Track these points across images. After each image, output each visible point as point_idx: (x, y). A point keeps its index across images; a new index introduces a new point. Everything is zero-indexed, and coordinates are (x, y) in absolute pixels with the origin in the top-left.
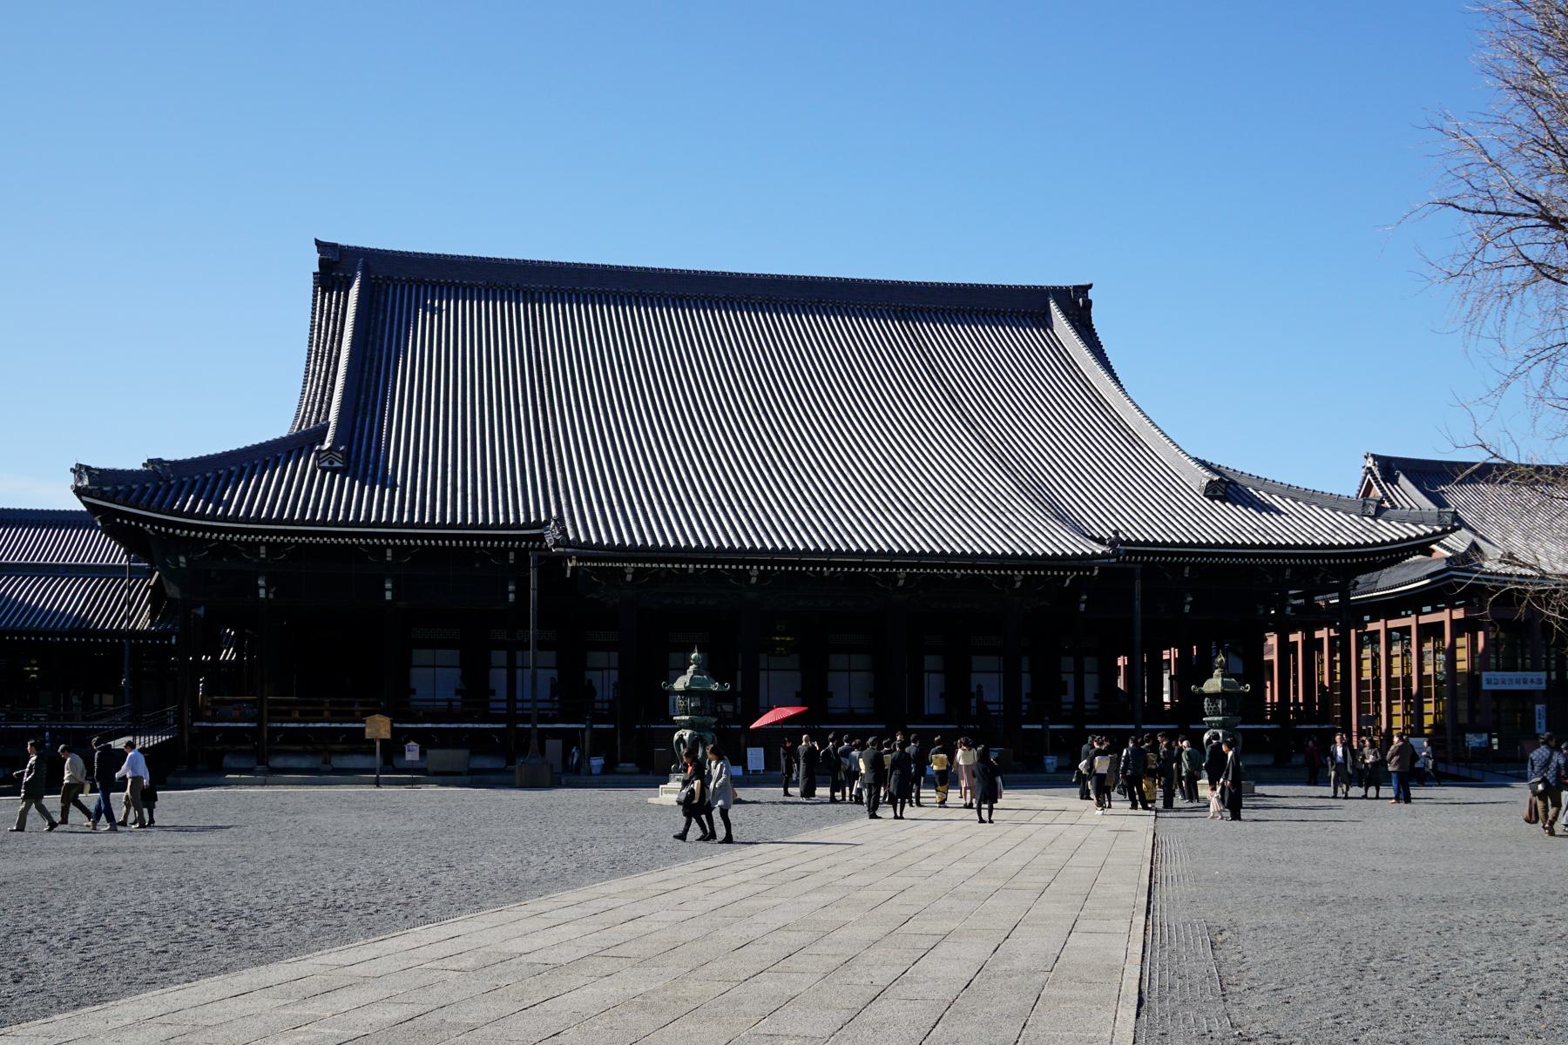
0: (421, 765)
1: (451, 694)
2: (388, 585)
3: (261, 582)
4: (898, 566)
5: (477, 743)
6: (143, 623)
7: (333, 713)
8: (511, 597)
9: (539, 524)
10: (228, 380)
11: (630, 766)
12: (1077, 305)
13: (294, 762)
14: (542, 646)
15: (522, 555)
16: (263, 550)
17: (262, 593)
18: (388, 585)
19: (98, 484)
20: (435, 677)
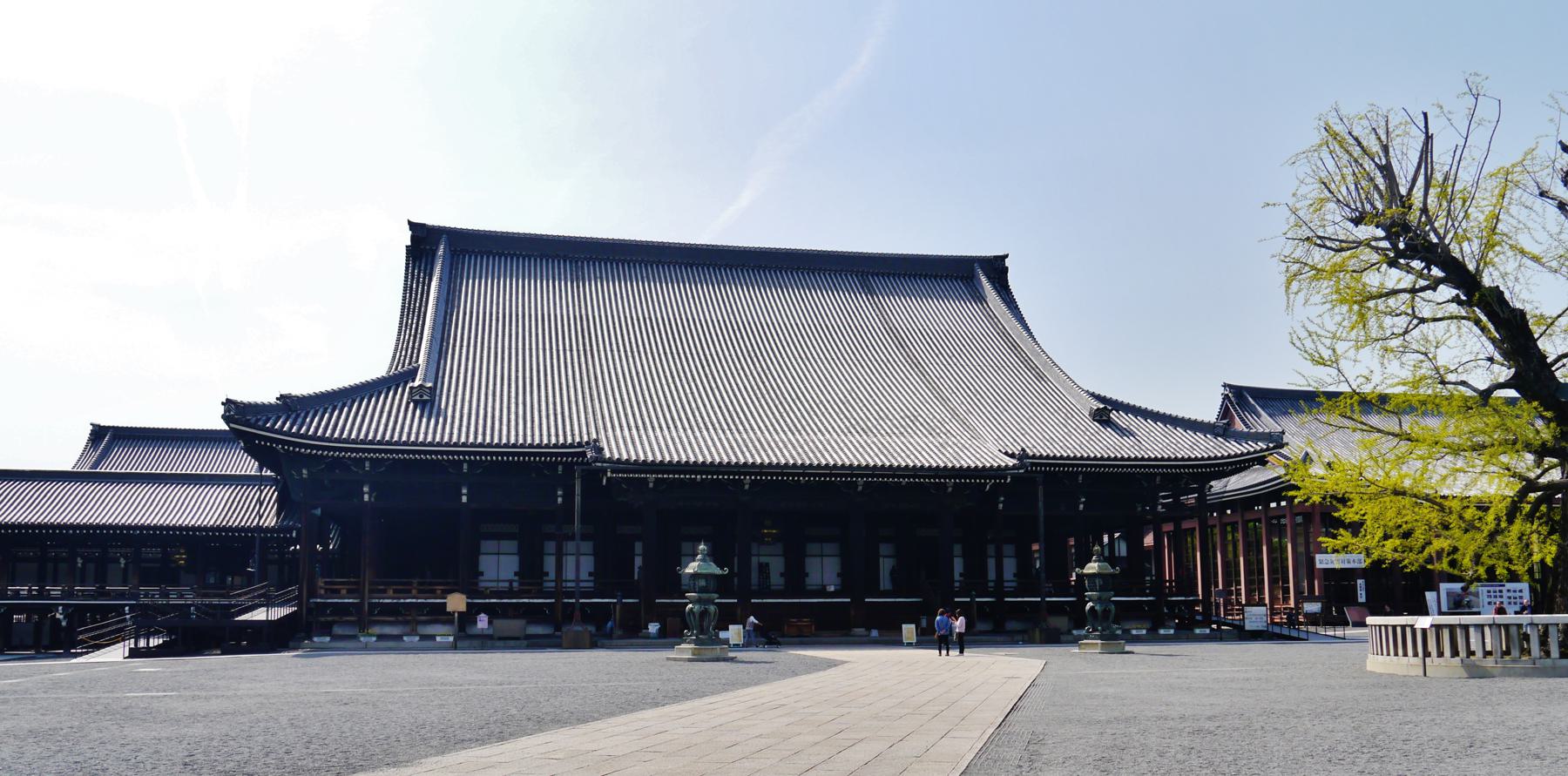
0: (491, 632)
1: (511, 576)
2: (464, 491)
4: (857, 476)
5: (532, 614)
6: (270, 520)
7: (420, 591)
9: (580, 445)
10: (332, 333)
12: (996, 269)
14: (584, 538)
15: (569, 467)
17: (366, 497)
18: (464, 491)
19: (235, 411)
20: (499, 566)
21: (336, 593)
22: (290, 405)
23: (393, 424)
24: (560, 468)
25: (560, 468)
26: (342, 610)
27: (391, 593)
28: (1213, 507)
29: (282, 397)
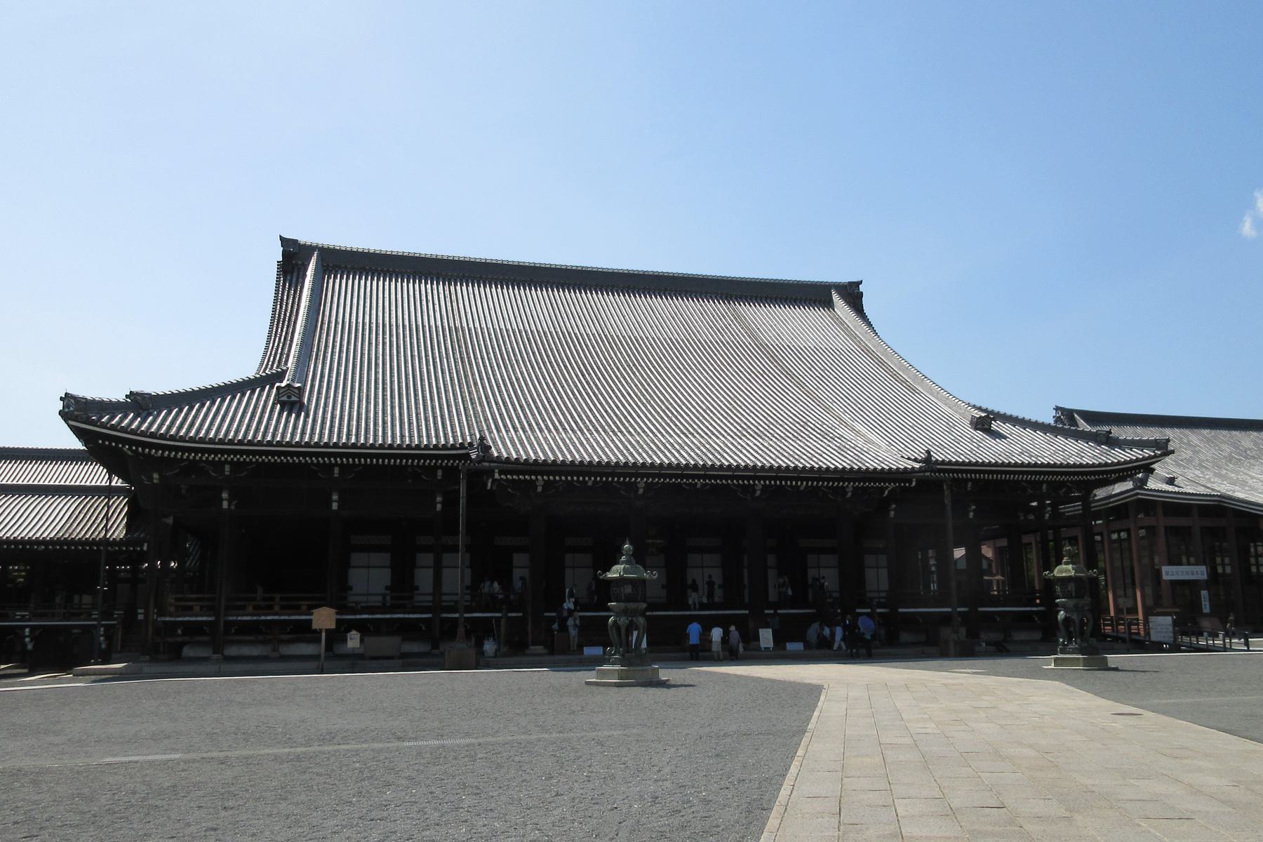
0: (361, 651)
2: (335, 497)
3: (225, 495)
5: (406, 630)
6: (118, 531)
7: (283, 608)
8: (439, 507)
10: (194, 337)
11: (539, 649)
13: (246, 651)
16: (227, 468)
17: (225, 505)
18: (335, 497)
19: (77, 411)
20: (370, 577)
21: (188, 610)
22: (141, 403)
23: (255, 422)
24: (440, 473)
25: (440, 473)
26: (194, 630)
27: (250, 609)
28: (1097, 515)
29: (132, 395)
